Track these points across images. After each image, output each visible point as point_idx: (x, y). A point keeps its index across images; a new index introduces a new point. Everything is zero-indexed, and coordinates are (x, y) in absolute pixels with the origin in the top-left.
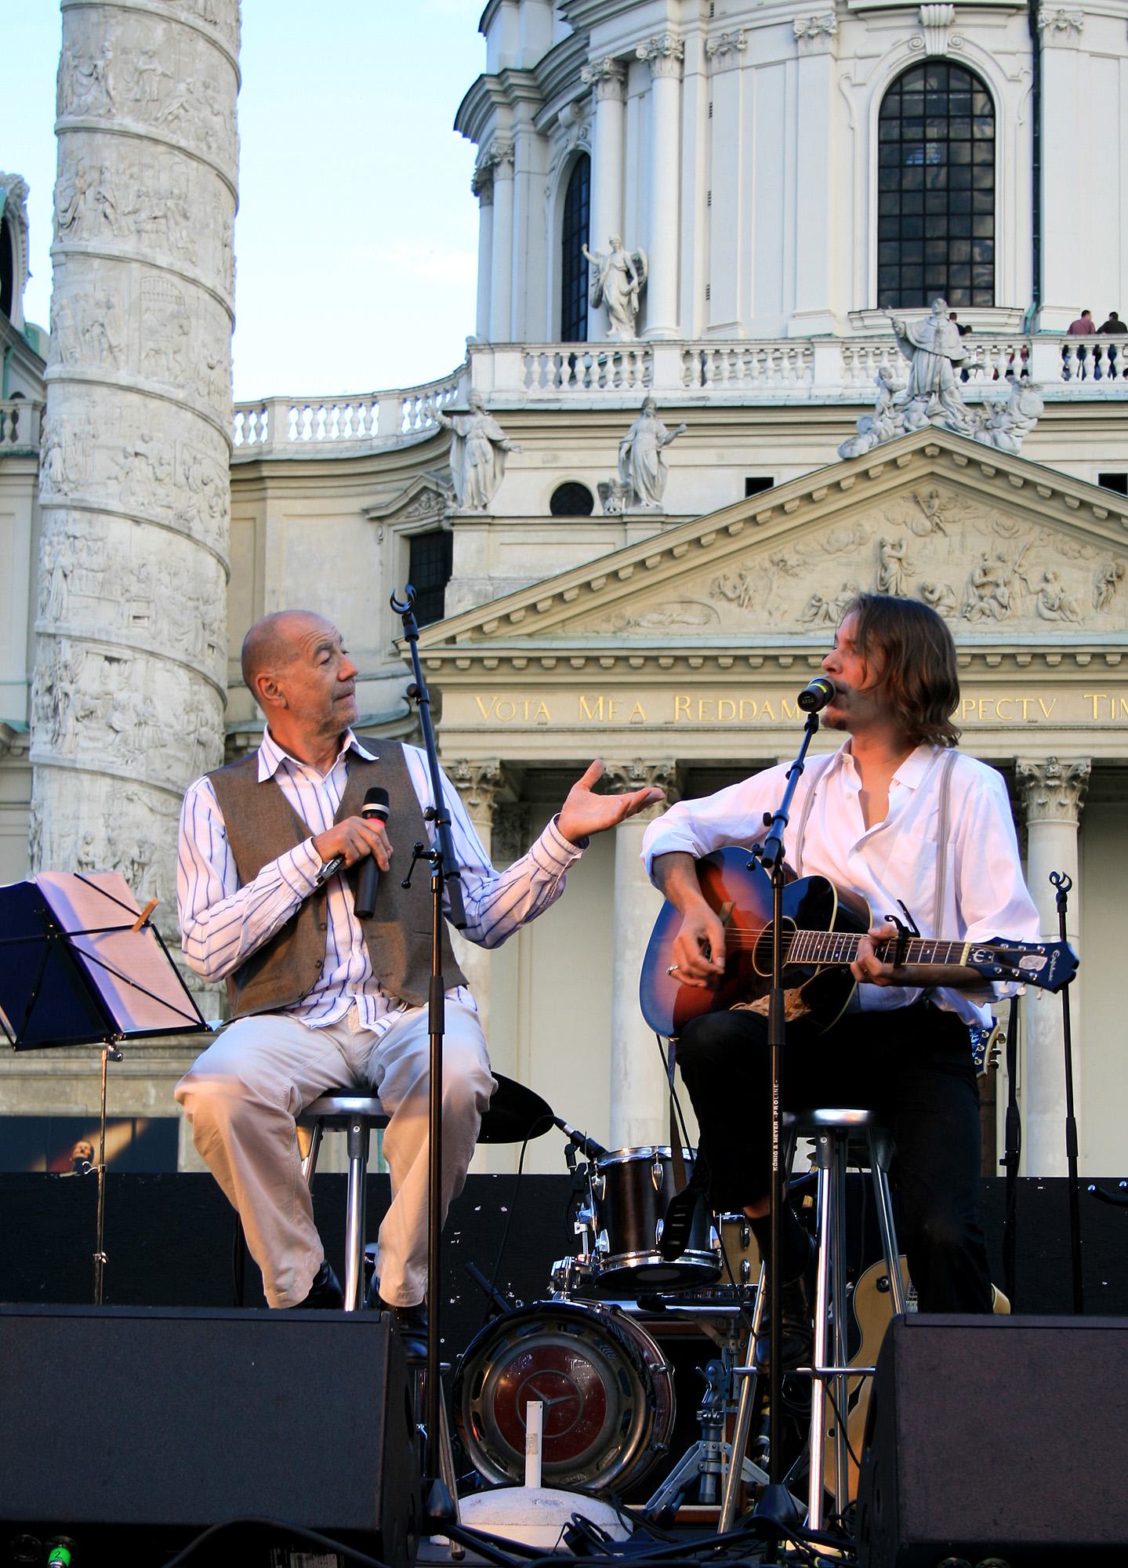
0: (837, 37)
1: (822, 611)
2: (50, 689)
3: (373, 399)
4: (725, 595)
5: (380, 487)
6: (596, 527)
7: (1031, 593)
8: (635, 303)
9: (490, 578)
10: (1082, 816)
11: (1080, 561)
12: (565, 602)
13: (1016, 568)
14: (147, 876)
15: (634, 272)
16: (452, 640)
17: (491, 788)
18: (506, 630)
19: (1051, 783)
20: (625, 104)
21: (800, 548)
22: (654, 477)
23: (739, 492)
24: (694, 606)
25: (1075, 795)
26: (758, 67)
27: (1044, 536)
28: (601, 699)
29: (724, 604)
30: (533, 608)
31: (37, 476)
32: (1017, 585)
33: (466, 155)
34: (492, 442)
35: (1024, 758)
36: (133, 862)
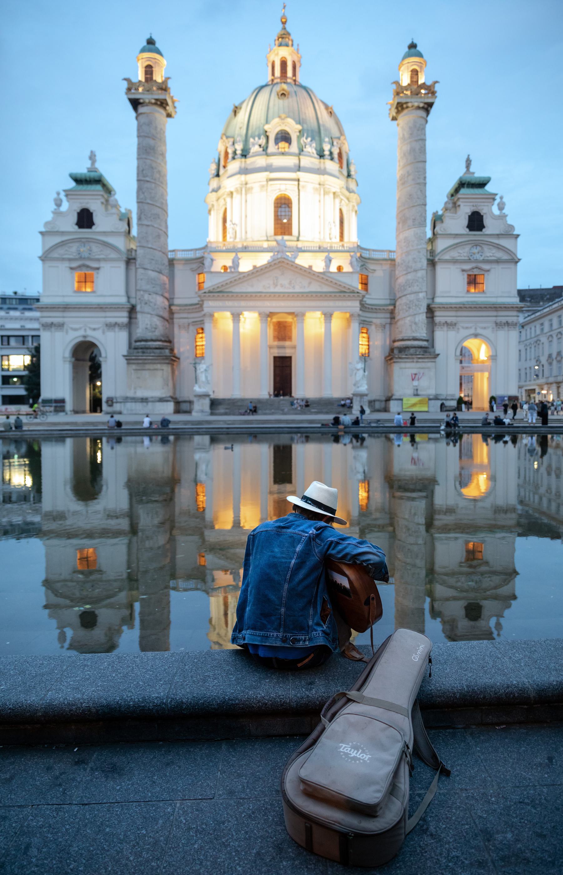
3: (191, 250)
14: (157, 331)
31: (135, 263)
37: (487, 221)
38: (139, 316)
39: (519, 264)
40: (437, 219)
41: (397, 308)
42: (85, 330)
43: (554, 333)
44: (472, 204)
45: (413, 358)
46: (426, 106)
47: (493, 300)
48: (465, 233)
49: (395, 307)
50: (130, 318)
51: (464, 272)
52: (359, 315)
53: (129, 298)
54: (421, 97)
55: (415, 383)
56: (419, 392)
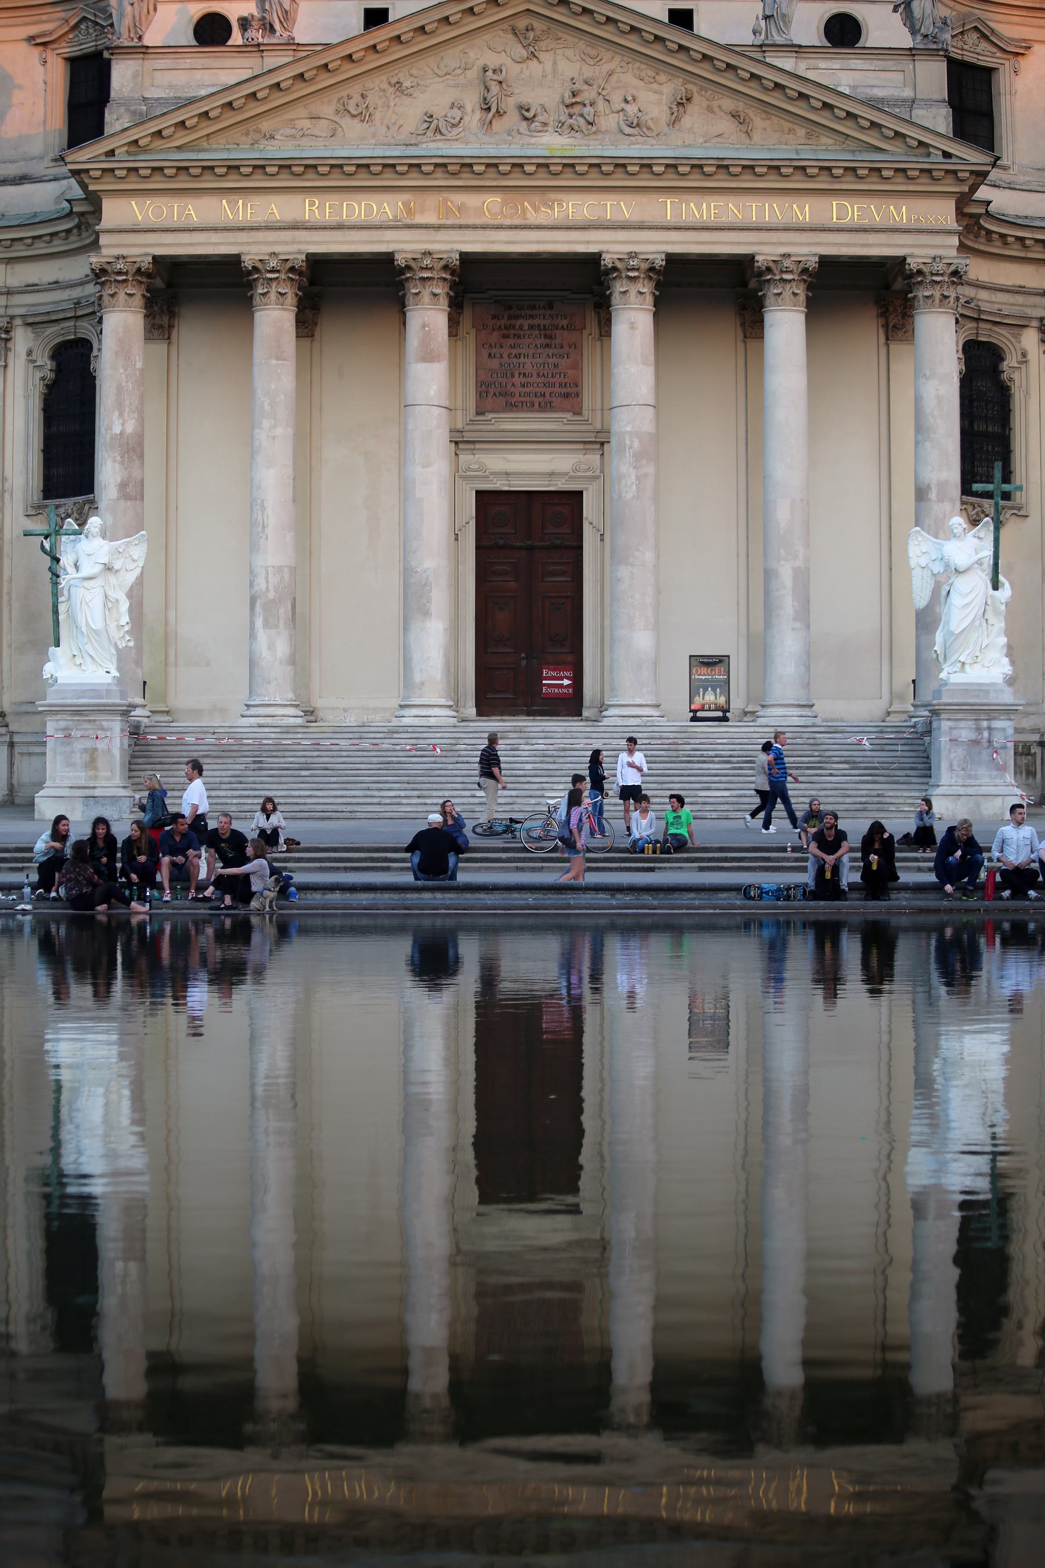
1: (433, 126)
4: (348, 112)
5: (44, 17)
6: (236, 55)
7: (613, 112)
9: (145, 99)
10: (657, 302)
11: (655, 86)
12: (210, 119)
13: (600, 91)
16: (111, 153)
17: (145, 280)
18: (158, 143)
19: (632, 274)
21: (414, 72)
22: (286, 12)
23: (357, 22)
24: (322, 120)
25: (652, 284)
27: (624, 64)
28: (241, 202)
29: (346, 122)
32: (601, 105)
35: (607, 252)
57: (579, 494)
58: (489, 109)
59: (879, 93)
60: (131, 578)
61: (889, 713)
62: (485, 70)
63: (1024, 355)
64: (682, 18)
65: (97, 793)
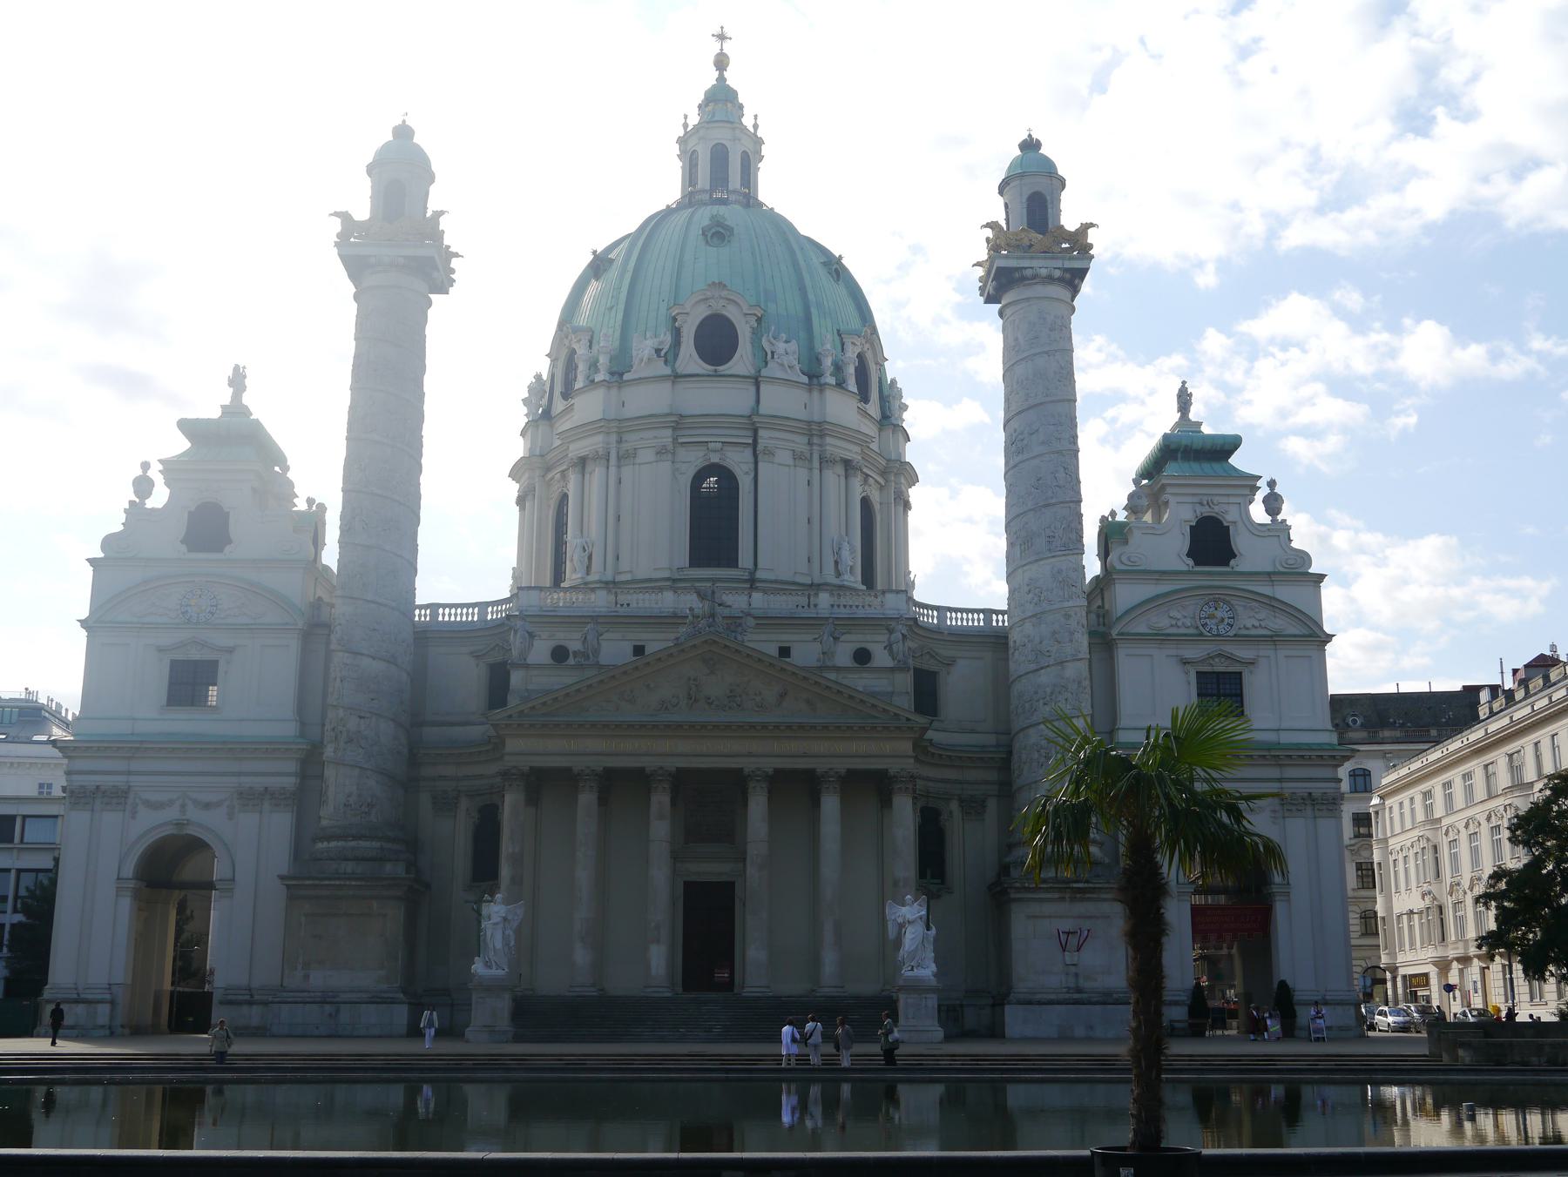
0: (674, 454)
2: (333, 729)
3: (473, 605)
8: (586, 560)
9: (527, 690)
10: (769, 792)
15: (586, 548)
16: (510, 716)
20: (584, 475)
23: (630, 650)
26: (639, 464)
30: (544, 704)
31: (329, 635)
33: (513, 488)
34: (528, 632)
36: (368, 805)
37: (1240, 541)
38: (329, 772)
39: (1328, 647)
40: (1111, 533)
41: (1015, 757)
42: (183, 806)
43: (1458, 820)
44: (1196, 499)
45: (1060, 890)
46: (1068, 276)
47: (1270, 737)
48: (1185, 568)
49: (1010, 753)
50: (303, 776)
51: (1188, 667)
52: (913, 778)
53: (303, 724)
54: (1053, 258)
55: (1068, 957)
56: (1082, 983)
57: (733, 883)
58: (691, 699)
59: (877, 689)
60: (515, 924)
61: (883, 991)
62: (689, 679)
63: (951, 812)
64: (785, 652)
65: (497, 1029)
